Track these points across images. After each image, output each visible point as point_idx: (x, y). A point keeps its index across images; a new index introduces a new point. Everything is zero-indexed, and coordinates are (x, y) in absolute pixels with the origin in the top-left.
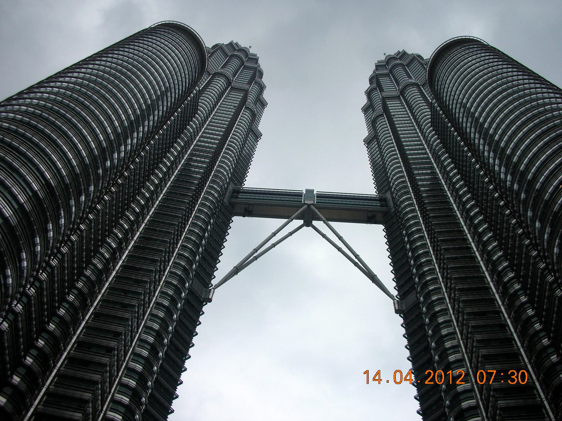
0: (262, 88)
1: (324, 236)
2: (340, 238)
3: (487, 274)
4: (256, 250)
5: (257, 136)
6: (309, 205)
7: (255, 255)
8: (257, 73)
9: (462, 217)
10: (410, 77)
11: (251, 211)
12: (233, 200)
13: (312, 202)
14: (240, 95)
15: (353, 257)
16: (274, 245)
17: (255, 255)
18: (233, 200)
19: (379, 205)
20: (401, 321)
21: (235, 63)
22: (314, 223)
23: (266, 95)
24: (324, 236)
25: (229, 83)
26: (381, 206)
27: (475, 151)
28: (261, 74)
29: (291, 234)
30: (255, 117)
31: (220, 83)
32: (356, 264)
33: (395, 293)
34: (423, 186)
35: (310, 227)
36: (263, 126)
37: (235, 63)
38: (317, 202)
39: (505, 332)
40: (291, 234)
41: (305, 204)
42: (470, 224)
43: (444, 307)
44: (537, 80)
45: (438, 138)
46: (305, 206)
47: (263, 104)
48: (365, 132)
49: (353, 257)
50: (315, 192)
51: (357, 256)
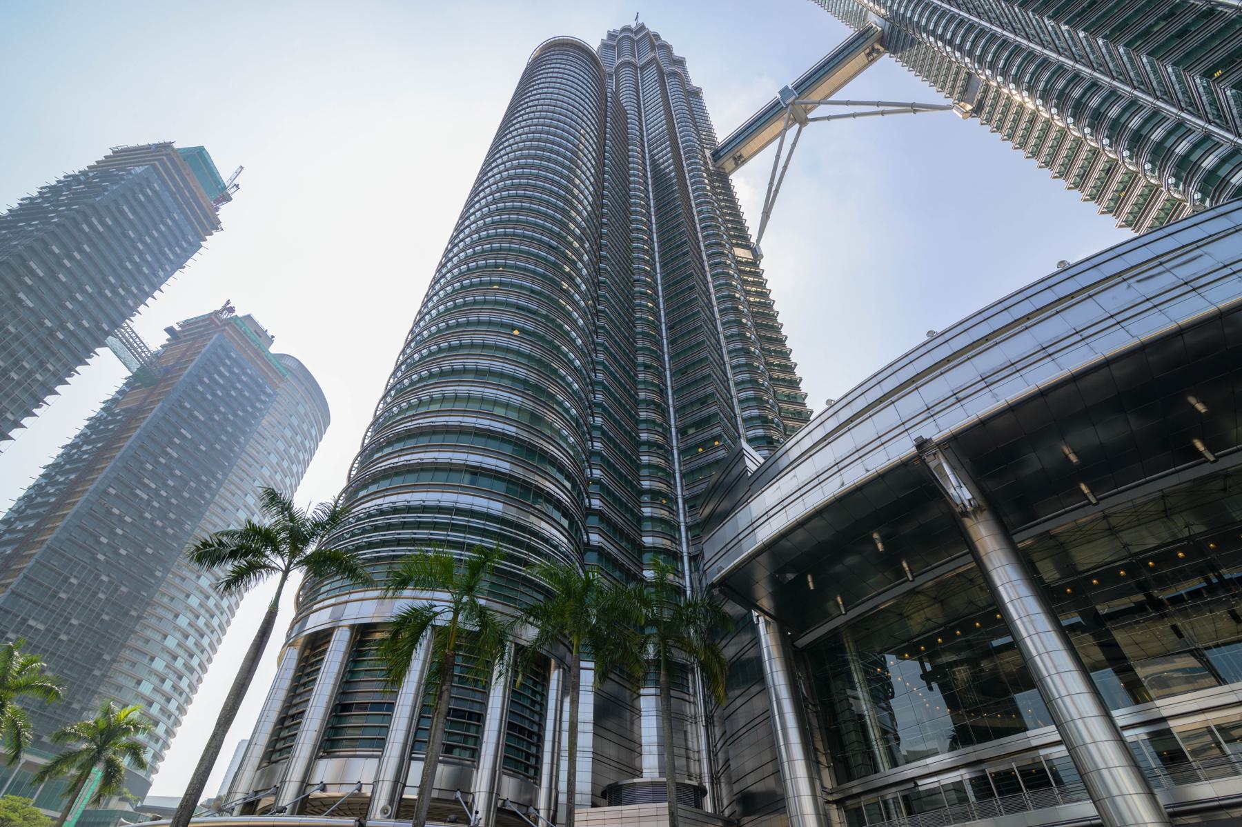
0: (667, 48)
1: (829, 118)
2: (847, 103)
4: (771, 184)
5: (696, 94)
6: (793, 103)
7: (773, 189)
8: (654, 42)
11: (740, 156)
13: (794, 97)
14: (653, 68)
15: (874, 108)
16: (785, 167)
17: (773, 189)
21: (626, 44)
22: (810, 116)
23: (677, 53)
24: (829, 118)
25: (636, 67)
28: (657, 36)
29: (794, 145)
30: (682, 79)
31: (626, 73)
32: (883, 113)
33: (950, 101)
35: (811, 124)
36: (695, 82)
37: (626, 44)
40: (794, 145)
47: (680, 62)
49: (874, 108)
50: (790, 87)
51: (878, 104)
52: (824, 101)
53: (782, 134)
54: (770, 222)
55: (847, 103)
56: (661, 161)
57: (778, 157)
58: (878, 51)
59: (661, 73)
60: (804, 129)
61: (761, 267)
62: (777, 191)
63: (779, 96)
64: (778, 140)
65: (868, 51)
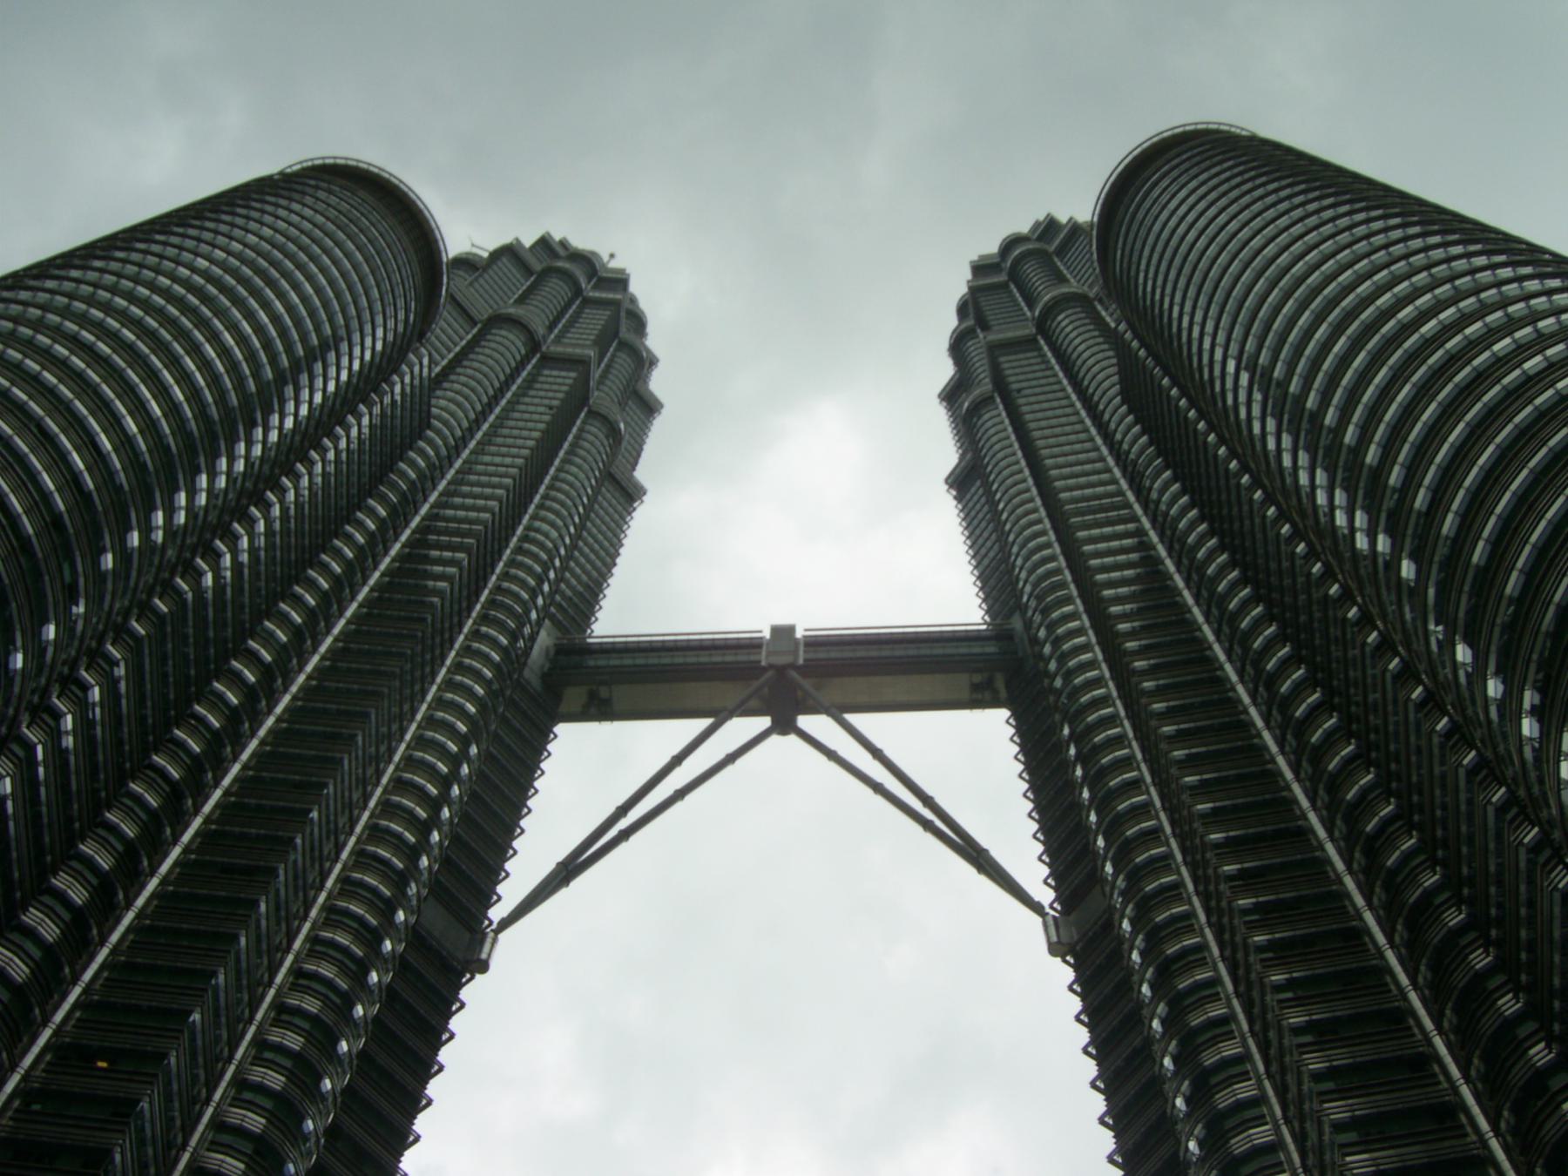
1: (831, 755)
3: (1313, 818)
6: (781, 670)
9: (1268, 726)
10: (1062, 280)
24: (831, 755)
27: (1320, 534)
34: (1118, 600)
35: (792, 739)
38: (805, 660)
39: (1381, 993)
41: (771, 666)
42: (1298, 745)
43: (1207, 975)
44: (1453, 232)
45: (1175, 479)
50: (799, 634)
52: (837, 712)
53: (721, 716)
54: (563, 895)
55: (877, 754)
56: (438, 569)
57: (677, 760)
58: (995, 692)
59: (578, 400)
60: (775, 739)
61: (464, 994)
62: (625, 835)
63: (767, 634)
64: (705, 722)
65: (977, 678)
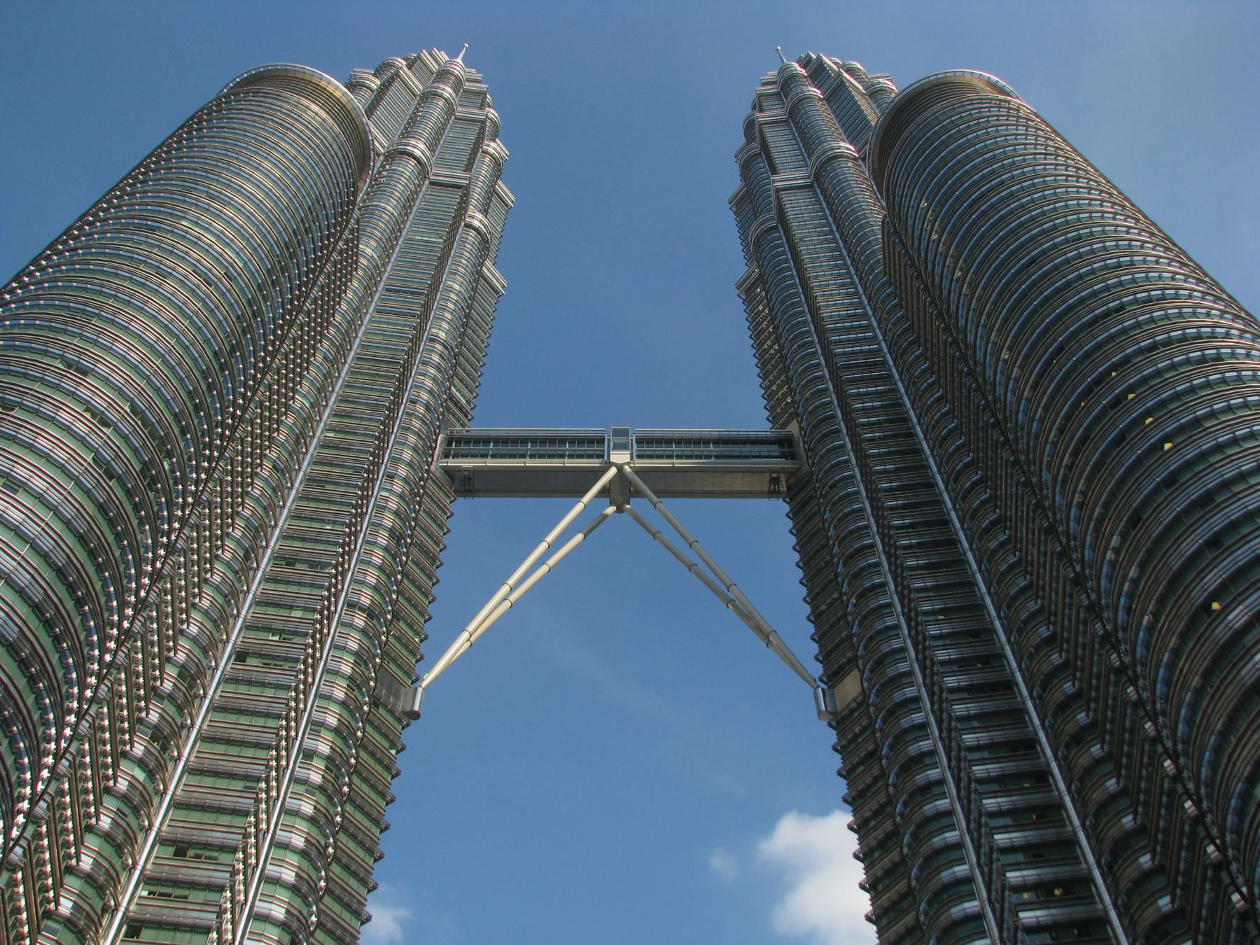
6: (620, 468)
12: (452, 462)
18: (452, 462)
19: (777, 454)
20: (832, 736)
26: (783, 456)
33: (817, 670)
46: (613, 471)
48: (736, 265)
